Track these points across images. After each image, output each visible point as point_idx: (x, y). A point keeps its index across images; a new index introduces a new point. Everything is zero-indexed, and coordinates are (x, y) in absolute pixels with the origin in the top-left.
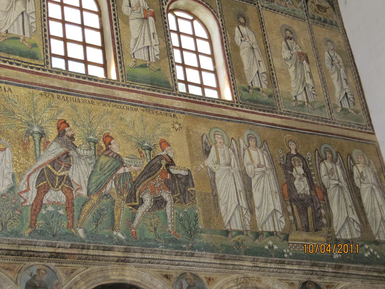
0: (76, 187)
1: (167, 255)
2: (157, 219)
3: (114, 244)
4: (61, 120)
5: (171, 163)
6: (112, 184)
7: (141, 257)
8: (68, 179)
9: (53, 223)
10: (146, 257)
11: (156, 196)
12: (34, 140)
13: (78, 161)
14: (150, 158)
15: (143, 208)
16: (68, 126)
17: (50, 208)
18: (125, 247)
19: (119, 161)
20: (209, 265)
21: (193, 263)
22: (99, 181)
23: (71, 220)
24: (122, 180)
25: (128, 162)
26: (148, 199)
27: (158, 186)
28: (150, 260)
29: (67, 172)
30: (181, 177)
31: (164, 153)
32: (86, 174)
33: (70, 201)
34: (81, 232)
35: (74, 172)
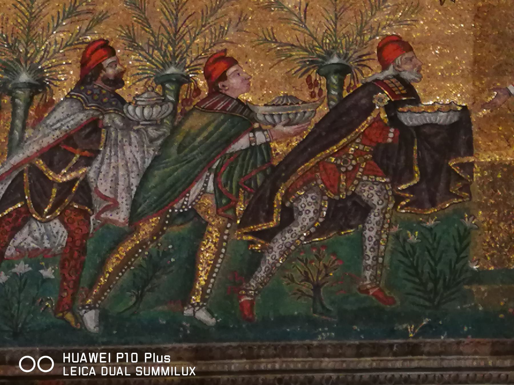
0: (98, 204)
1: (329, 356)
2: (328, 259)
3: (180, 342)
4: (94, 42)
5: (406, 94)
6: (206, 182)
7: (247, 367)
8: (85, 187)
9: (19, 303)
10: (262, 367)
11: (337, 198)
12: (15, 106)
13: (120, 138)
14: (340, 94)
15: (288, 235)
16: (112, 52)
17: (22, 268)
18: (194, 345)
19: (243, 117)
20: (479, 374)
21: (423, 373)
22: (169, 181)
23: (71, 291)
24: (238, 168)
25: (269, 118)
26: (309, 209)
27: (350, 168)
28: (279, 376)
29: (84, 170)
30: (434, 131)
31: (390, 72)
32: (135, 168)
33: (78, 243)
34: (90, 319)
35: (104, 167)
